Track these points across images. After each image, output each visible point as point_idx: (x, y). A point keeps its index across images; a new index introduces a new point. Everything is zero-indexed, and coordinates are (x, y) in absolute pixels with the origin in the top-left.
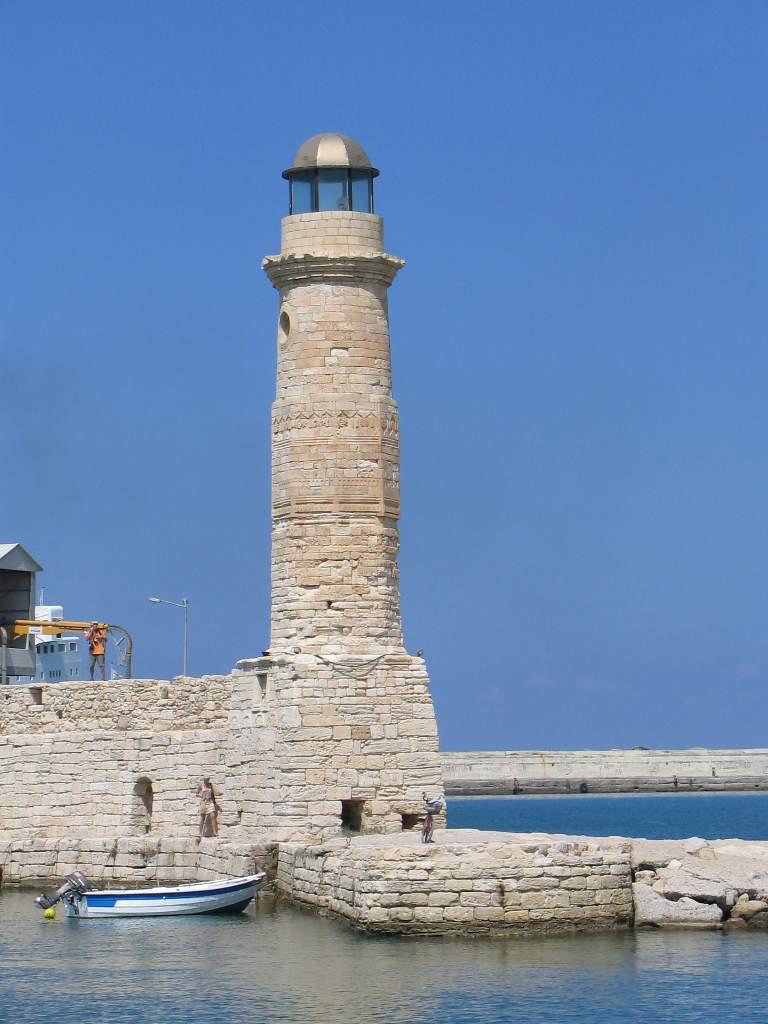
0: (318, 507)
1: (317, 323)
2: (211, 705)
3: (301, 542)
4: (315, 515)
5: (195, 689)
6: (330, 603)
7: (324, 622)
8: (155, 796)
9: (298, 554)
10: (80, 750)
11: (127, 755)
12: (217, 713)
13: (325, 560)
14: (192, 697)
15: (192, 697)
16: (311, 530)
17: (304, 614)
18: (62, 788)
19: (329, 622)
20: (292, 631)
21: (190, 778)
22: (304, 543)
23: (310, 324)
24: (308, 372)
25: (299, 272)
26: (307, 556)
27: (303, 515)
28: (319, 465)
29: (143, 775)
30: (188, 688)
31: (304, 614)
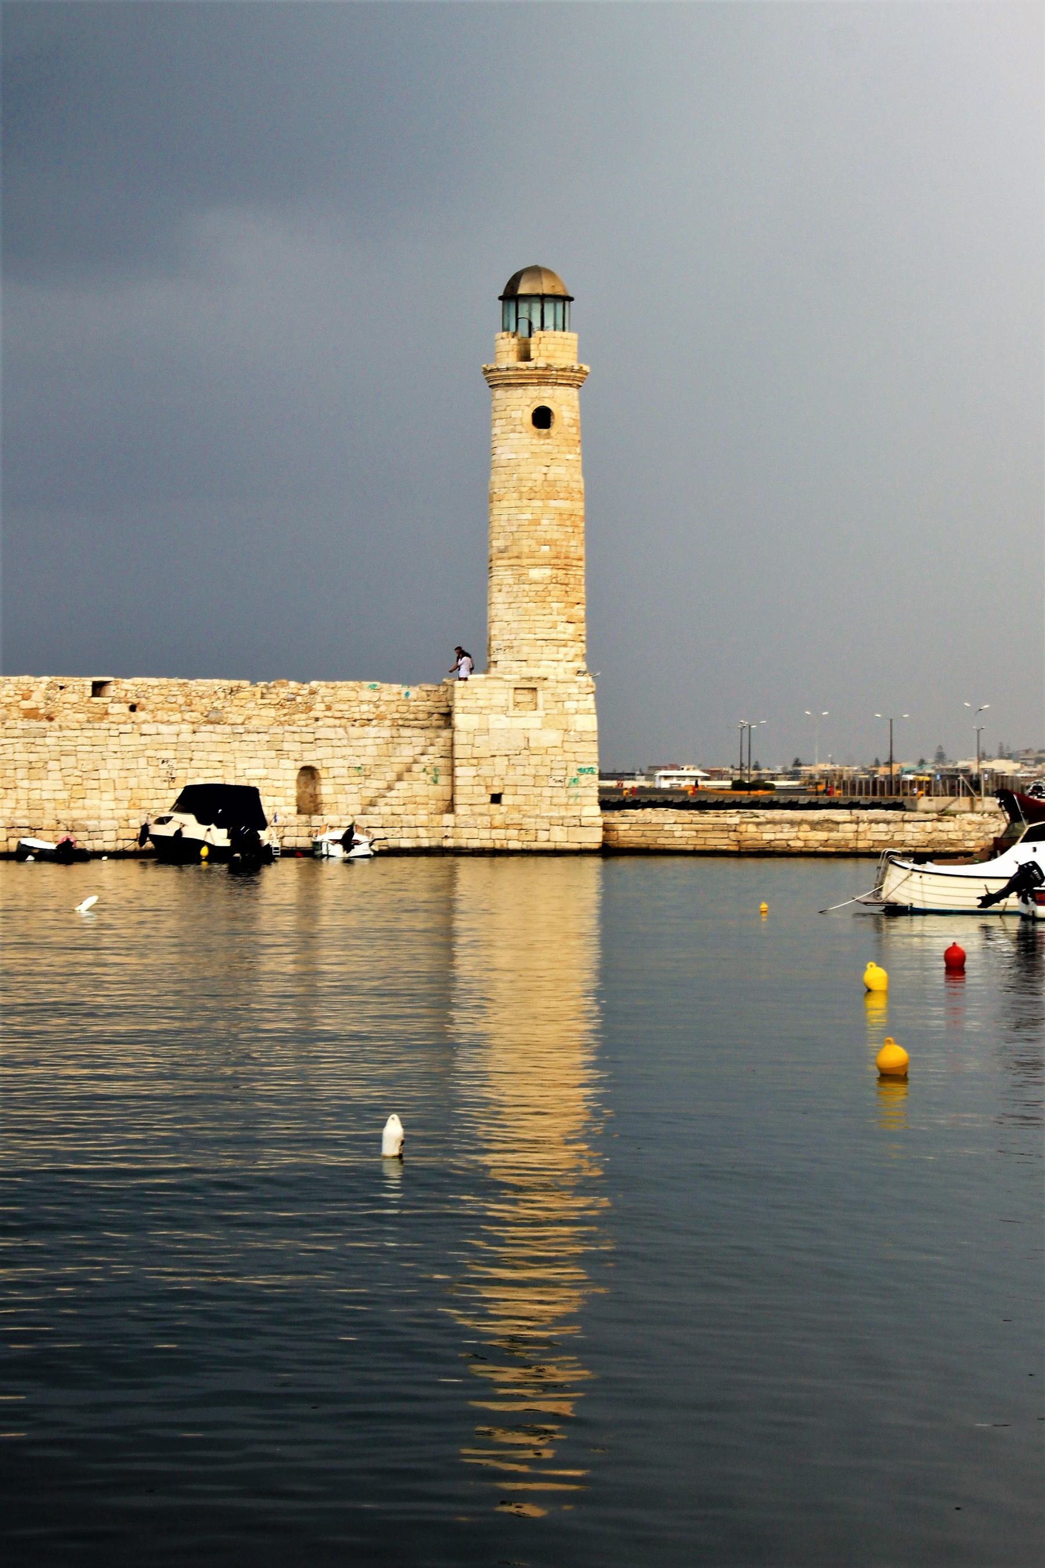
0: (575, 563)
2: (322, 707)
3: (568, 589)
4: (574, 568)
5: (302, 692)
8: (324, 782)
9: (566, 599)
10: (229, 740)
11: (286, 746)
13: (578, 604)
14: (299, 699)
15: (299, 699)
16: (572, 580)
20: (560, 656)
21: (363, 767)
24: (569, 457)
27: (568, 567)
29: (308, 764)
30: (295, 691)
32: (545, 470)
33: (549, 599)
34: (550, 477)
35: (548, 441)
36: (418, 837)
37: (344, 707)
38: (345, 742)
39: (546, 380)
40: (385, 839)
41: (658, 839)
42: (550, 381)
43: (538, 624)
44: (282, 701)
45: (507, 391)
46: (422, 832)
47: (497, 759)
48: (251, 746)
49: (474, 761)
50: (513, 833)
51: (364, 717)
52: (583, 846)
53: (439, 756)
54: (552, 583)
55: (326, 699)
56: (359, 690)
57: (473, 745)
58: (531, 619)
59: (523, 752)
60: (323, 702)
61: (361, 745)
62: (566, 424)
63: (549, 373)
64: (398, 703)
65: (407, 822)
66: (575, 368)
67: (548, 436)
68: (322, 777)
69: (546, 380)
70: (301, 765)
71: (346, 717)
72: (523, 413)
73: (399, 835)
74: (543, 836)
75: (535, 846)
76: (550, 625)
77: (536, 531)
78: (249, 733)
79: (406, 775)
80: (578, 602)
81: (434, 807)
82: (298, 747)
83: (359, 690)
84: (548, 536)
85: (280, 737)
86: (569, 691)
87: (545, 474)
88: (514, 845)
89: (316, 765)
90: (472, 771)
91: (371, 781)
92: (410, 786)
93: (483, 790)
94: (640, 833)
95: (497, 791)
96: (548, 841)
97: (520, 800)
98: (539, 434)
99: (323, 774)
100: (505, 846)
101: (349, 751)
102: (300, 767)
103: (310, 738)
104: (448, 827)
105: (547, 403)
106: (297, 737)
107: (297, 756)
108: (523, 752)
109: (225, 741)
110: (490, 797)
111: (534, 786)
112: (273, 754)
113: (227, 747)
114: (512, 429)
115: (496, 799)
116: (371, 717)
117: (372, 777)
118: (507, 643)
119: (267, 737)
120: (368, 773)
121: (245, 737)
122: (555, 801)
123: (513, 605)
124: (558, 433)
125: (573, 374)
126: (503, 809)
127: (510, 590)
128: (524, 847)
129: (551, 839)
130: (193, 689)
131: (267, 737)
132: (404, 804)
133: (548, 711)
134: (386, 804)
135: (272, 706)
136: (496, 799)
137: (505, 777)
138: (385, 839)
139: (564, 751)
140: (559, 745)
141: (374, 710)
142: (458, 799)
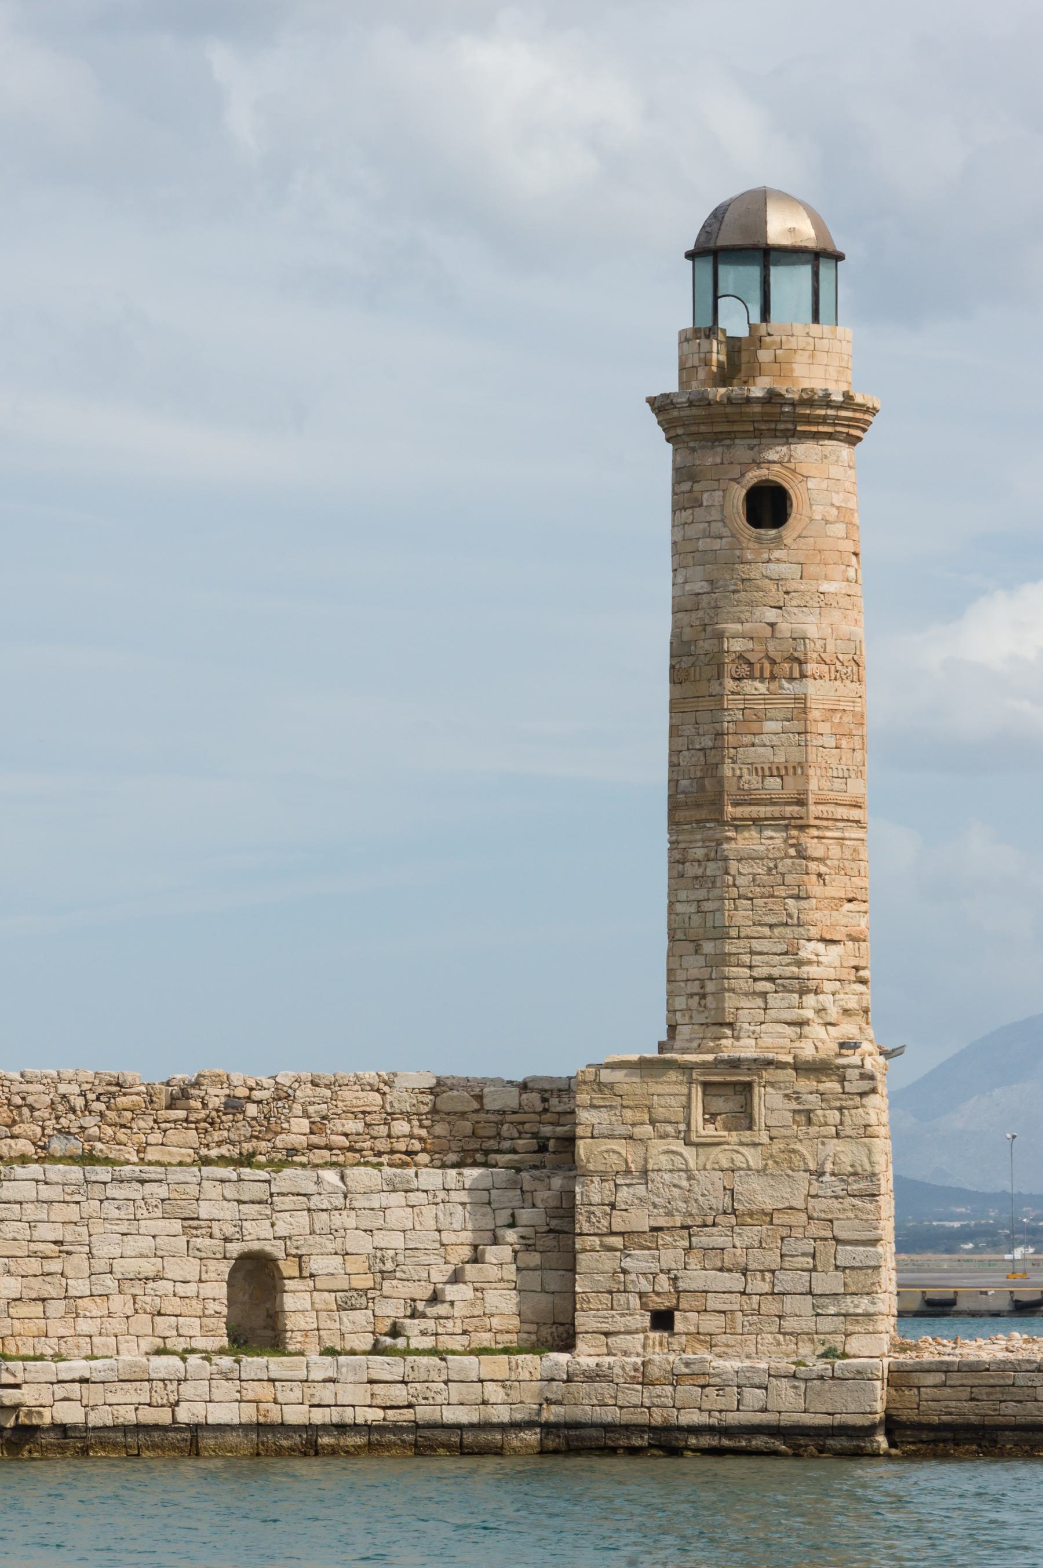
0: (841, 812)
1: (838, 508)
2: (304, 1125)
3: (823, 869)
4: (840, 824)
6: (857, 968)
7: (852, 1003)
8: (289, 1284)
10: (77, 1198)
11: (205, 1210)
12: (315, 1139)
13: (850, 901)
14: (252, 1110)
15: (252, 1110)
16: (835, 851)
17: (828, 986)
18: (34, 1266)
19: (859, 1002)
21: (379, 1254)
22: (828, 871)
23: (828, 508)
25: (824, 420)
26: (832, 891)
27: (825, 823)
28: (844, 743)
29: (256, 1246)
31: (828, 986)
32: (771, 615)
33: (781, 891)
34: (785, 628)
35: (777, 554)
36: (484, 1403)
37: (354, 1126)
38: (339, 1201)
39: (773, 426)
40: (410, 1406)
41: (1003, 1405)
42: (782, 426)
43: (757, 945)
44: (214, 1114)
45: (693, 450)
46: (494, 1392)
47: (666, 1238)
48: (127, 1212)
49: (617, 1241)
50: (688, 1392)
51: (401, 1146)
52: (838, 1419)
53: (546, 1228)
54: (787, 856)
55: (311, 1109)
56: (386, 1089)
57: (613, 1206)
58: (742, 935)
59: (720, 1219)
60: (306, 1115)
61: (377, 1205)
62: (818, 517)
63: (778, 410)
64: (475, 1117)
65: (461, 1370)
66: (833, 398)
67: (778, 542)
68: (285, 1274)
69: (773, 426)
70: (235, 1249)
71: (358, 1146)
72: (724, 497)
73: (439, 1399)
74: (754, 1397)
75: (733, 1418)
76: (782, 947)
77: (753, 745)
78: (122, 1181)
79: (471, 1271)
80: (850, 896)
81: (534, 1337)
82: (229, 1211)
83: (386, 1089)
84: (780, 759)
85: (193, 1190)
86: (822, 1087)
87: (772, 625)
88: (692, 1417)
89: (276, 1249)
90: (608, 1262)
91: (395, 1282)
92: (479, 1294)
93: (635, 1302)
94: (965, 1394)
95: (662, 1303)
96: (764, 1410)
97: (712, 1323)
98: (759, 540)
99: (288, 1268)
100: (673, 1421)
101: (349, 1220)
102: (235, 1255)
103: (259, 1191)
104: (553, 1380)
105: (774, 473)
106: (230, 1191)
107: (230, 1230)
108: (720, 1219)
109: (68, 1198)
110: (648, 1316)
111: (743, 1293)
112: (177, 1226)
113: (72, 1212)
114: (704, 530)
115: (662, 1320)
116: (417, 1146)
117: (398, 1275)
118: (695, 988)
119: (162, 1191)
120: (389, 1266)
121: (112, 1191)
122: (789, 1324)
123: (708, 906)
124: (799, 536)
125: (831, 412)
126: (676, 1342)
127: (700, 872)
128: (713, 1421)
129: (769, 1407)
130: (14, 1089)
131: (162, 1191)
132: (465, 1332)
133: (774, 1132)
134: (423, 1333)
135: (193, 1126)
136: (662, 1320)
137: (680, 1274)
138: (410, 1406)
139: (810, 1218)
140: (799, 1204)
141: (423, 1133)
142: (584, 1321)
